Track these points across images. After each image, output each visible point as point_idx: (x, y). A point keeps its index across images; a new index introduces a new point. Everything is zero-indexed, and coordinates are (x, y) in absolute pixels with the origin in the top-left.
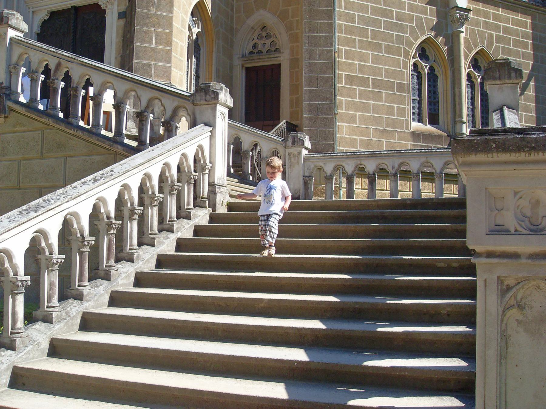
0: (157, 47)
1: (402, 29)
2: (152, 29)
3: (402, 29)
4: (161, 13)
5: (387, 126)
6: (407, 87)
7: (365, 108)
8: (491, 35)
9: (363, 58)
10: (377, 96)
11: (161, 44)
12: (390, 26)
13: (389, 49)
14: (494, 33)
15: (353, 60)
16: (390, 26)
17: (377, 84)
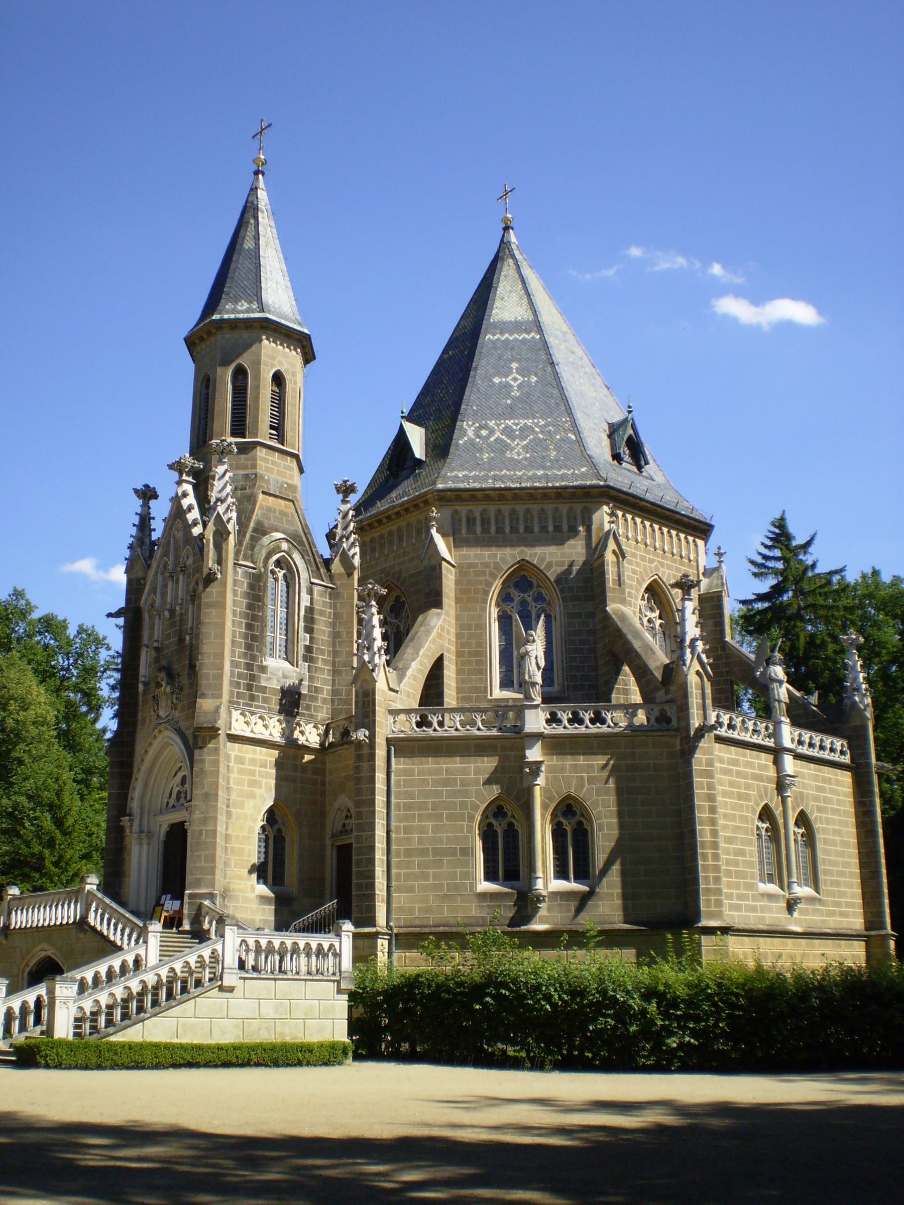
0: (207, 865)
1: (466, 794)
2: (201, 852)
3: (466, 794)
4: (208, 840)
5: (448, 890)
6: (472, 850)
7: (425, 877)
8: (582, 778)
9: (423, 830)
10: (439, 864)
11: (207, 863)
12: (455, 794)
13: (451, 817)
14: (585, 775)
15: (412, 833)
16: (455, 794)
17: (436, 852)
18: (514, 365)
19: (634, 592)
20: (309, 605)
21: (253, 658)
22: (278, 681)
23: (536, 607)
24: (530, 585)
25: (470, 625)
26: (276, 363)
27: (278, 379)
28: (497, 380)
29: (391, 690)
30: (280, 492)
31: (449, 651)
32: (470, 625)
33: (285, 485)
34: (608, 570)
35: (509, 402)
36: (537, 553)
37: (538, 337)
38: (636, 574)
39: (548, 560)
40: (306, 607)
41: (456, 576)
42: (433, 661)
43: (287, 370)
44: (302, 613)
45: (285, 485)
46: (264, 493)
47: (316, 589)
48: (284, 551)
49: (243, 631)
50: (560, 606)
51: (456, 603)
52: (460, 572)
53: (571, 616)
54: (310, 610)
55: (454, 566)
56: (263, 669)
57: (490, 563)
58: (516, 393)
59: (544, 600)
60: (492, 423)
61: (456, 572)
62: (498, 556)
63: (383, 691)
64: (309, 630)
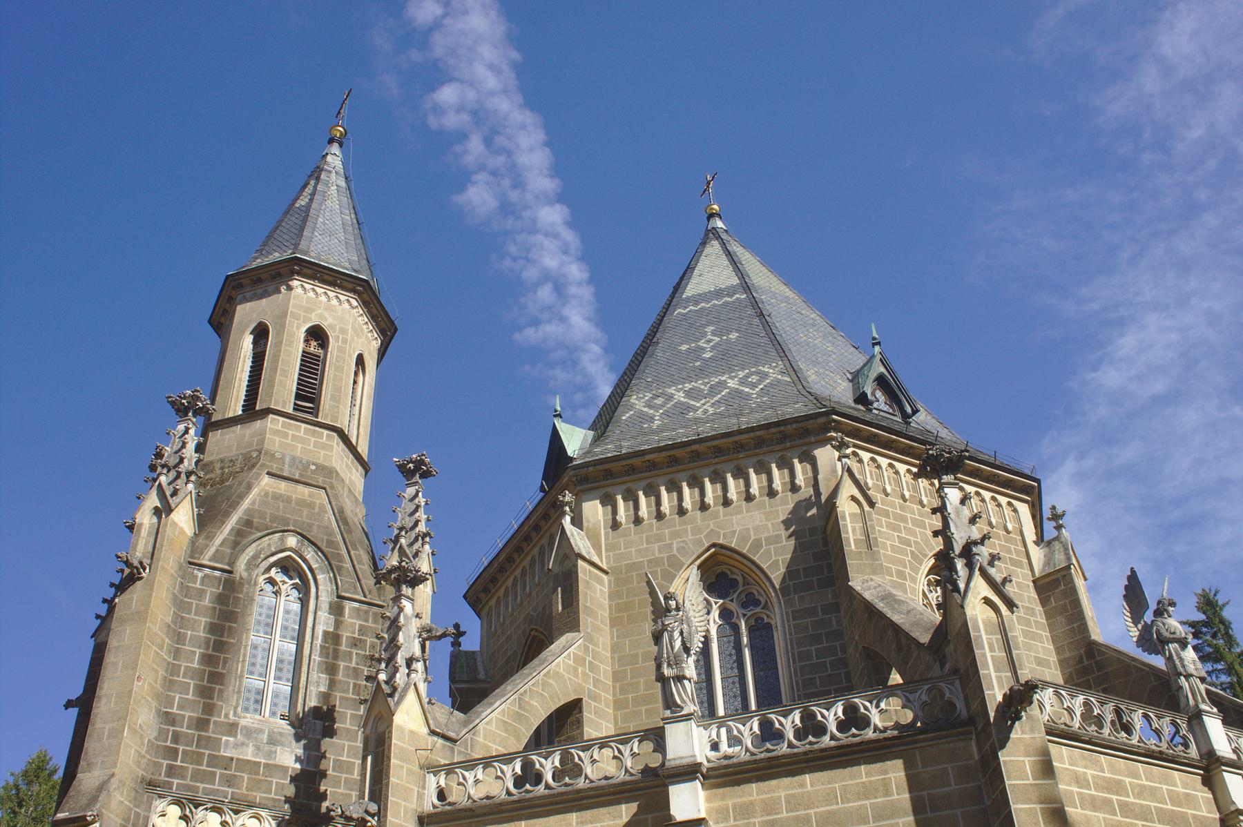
18: (710, 329)
19: (908, 570)
20: (331, 629)
21: (209, 709)
22: (258, 748)
23: (732, 601)
24: (734, 583)
25: (636, 656)
26: (313, 316)
27: (317, 334)
28: (684, 347)
29: (433, 733)
30: (301, 475)
31: (595, 698)
32: (636, 656)
33: (313, 467)
34: (846, 526)
35: (698, 363)
36: (735, 531)
37: (744, 296)
38: (910, 546)
39: (753, 538)
40: (326, 633)
41: (610, 587)
42: (553, 707)
43: (331, 326)
44: (319, 642)
45: (313, 467)
46: (268, 473)
47: (348, 606)
48: (290, 549)
49: (196, 665)
50: (780, 603)
51: (612, 626)
52: (617, 580)
53: (797, 615)
54: (332, 638)
55: (606, 573)
56: (232, 728)
57: (663, 558)
58: (707, 355)
59: (756, 603)
60: (672, 390)
61: (610, 581)
62: (675, 546)
63: (412, 732)
64: (331, 669)
